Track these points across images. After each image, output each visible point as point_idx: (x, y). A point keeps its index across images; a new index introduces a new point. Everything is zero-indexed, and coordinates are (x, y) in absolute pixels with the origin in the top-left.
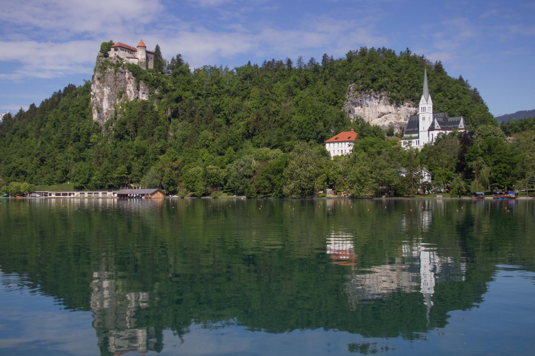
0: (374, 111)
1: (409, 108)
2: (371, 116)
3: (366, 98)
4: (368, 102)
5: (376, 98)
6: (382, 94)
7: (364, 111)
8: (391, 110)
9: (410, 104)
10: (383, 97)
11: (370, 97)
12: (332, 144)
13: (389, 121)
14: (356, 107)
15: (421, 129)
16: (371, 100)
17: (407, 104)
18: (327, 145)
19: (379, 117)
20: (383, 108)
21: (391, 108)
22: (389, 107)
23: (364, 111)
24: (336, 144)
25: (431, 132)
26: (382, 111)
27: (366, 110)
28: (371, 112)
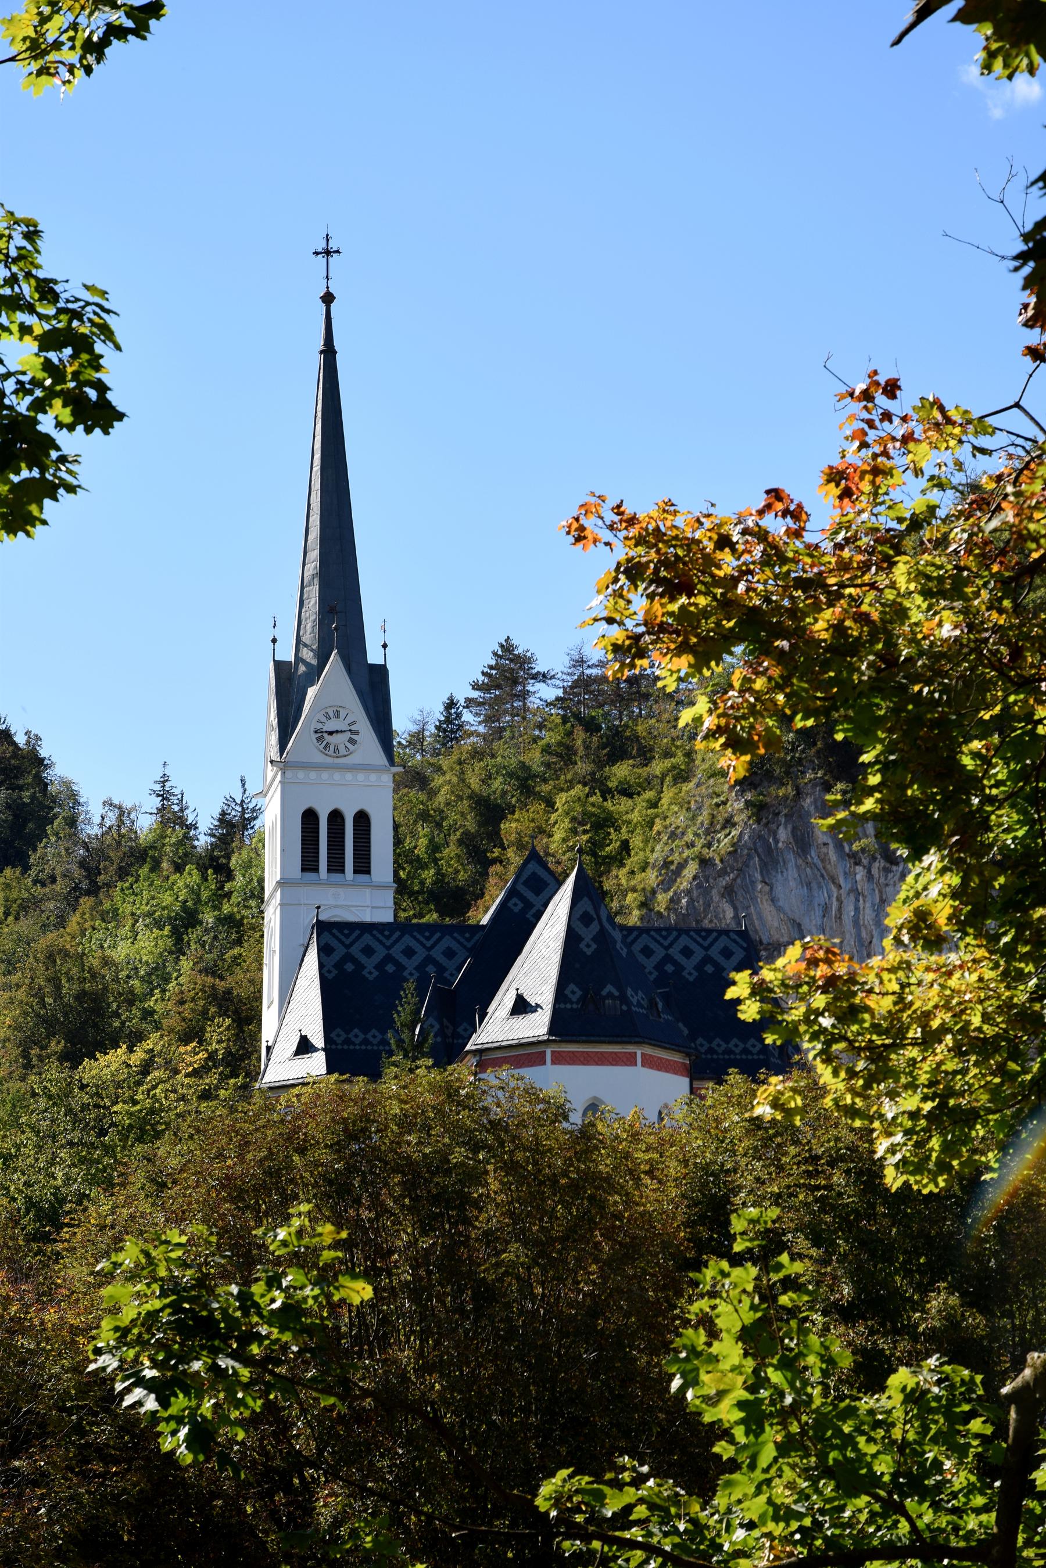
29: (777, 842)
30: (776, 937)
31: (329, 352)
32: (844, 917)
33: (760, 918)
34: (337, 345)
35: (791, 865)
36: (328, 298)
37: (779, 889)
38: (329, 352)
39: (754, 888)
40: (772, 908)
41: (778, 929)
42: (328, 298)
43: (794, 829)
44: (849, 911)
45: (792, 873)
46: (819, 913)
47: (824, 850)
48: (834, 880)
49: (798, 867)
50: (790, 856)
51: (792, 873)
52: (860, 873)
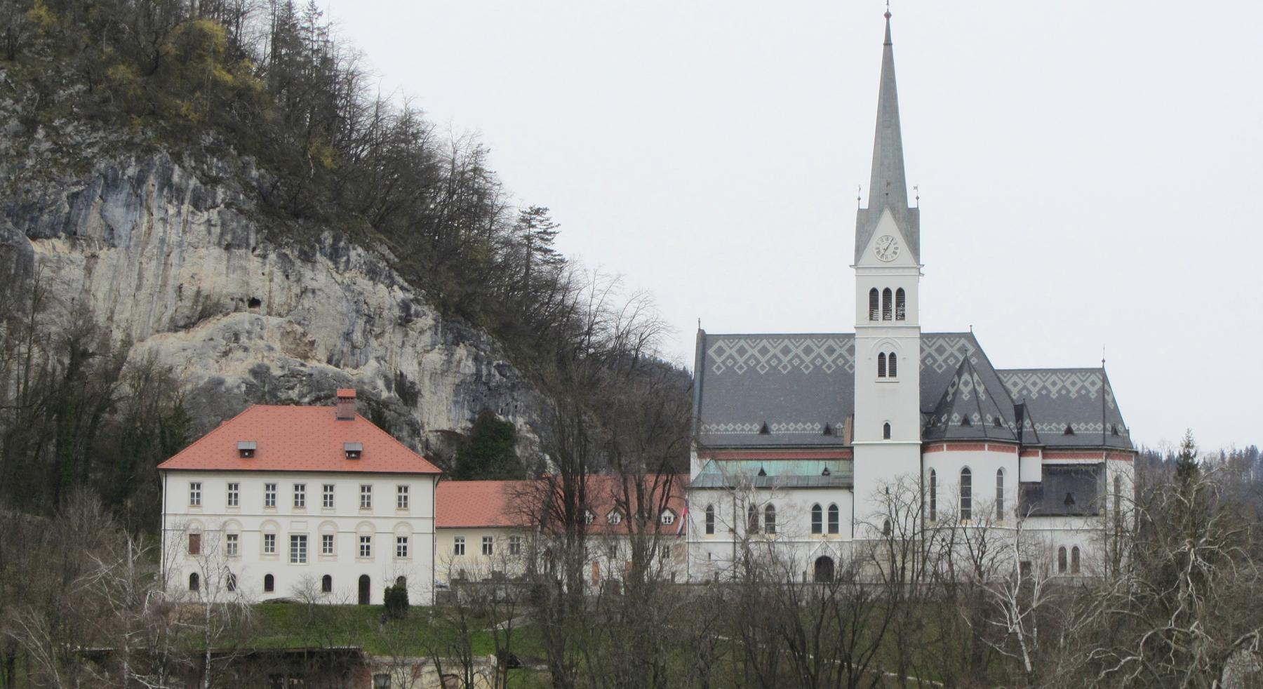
0: (149, 275)
1: (364, 283)
2: (124, 313)
3: (112, 184)
4: (117, 211)
5: (177, 194)
6: (215, 164)
7: (89, 271)
8: (259, 288)
9: (371, 257)
10: (220, 193)
11: (140, 181)
12: (215, 489)
13: (251, 361)
14: (34, 237)
15: (865, 430)
16: (138, 201)
17: (357, 254)
18: (175, 492)
19: (175, 327)
20: (210, 270)
21: (260, 273)
22: (254, 263)
23: (89, 271)
24: (252, 489)
25: (947, 462)
26: (206, 286)
27: (101, 268)
28: (126, 285)
29: (123, 174)
30: (90, 231)
31: (888, 44)
32: (153, 232)
33: (85, 219)
34: (893, 41)
35: (125, 191)
36: (888, 16)
37: (110, 205)
38: (888, 44)
39: (93, 199)
40: (98, 216)
41: (95, 229)
42: (888, 16)
43: (141, 171)
44: (159, 229)
45: (122, 197)
46: (130, 226)
47: (151, 188)
48: (149, 209)
49: (129, 194)
50: (127, 188)
51: (122, 197)
52: (172, 210)
